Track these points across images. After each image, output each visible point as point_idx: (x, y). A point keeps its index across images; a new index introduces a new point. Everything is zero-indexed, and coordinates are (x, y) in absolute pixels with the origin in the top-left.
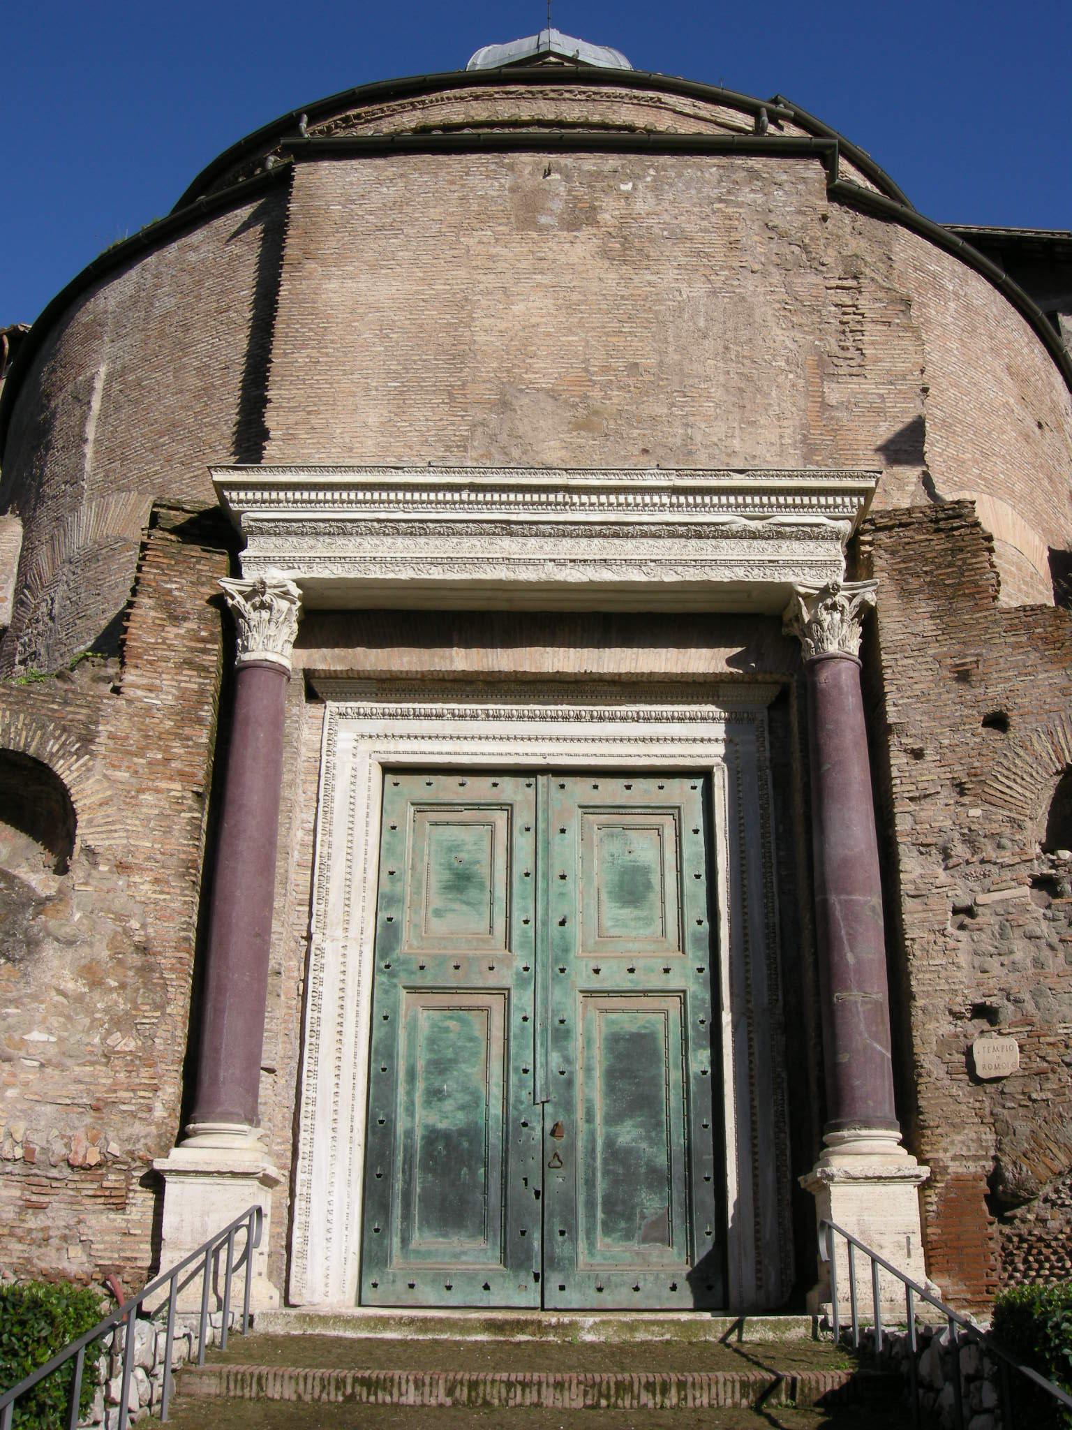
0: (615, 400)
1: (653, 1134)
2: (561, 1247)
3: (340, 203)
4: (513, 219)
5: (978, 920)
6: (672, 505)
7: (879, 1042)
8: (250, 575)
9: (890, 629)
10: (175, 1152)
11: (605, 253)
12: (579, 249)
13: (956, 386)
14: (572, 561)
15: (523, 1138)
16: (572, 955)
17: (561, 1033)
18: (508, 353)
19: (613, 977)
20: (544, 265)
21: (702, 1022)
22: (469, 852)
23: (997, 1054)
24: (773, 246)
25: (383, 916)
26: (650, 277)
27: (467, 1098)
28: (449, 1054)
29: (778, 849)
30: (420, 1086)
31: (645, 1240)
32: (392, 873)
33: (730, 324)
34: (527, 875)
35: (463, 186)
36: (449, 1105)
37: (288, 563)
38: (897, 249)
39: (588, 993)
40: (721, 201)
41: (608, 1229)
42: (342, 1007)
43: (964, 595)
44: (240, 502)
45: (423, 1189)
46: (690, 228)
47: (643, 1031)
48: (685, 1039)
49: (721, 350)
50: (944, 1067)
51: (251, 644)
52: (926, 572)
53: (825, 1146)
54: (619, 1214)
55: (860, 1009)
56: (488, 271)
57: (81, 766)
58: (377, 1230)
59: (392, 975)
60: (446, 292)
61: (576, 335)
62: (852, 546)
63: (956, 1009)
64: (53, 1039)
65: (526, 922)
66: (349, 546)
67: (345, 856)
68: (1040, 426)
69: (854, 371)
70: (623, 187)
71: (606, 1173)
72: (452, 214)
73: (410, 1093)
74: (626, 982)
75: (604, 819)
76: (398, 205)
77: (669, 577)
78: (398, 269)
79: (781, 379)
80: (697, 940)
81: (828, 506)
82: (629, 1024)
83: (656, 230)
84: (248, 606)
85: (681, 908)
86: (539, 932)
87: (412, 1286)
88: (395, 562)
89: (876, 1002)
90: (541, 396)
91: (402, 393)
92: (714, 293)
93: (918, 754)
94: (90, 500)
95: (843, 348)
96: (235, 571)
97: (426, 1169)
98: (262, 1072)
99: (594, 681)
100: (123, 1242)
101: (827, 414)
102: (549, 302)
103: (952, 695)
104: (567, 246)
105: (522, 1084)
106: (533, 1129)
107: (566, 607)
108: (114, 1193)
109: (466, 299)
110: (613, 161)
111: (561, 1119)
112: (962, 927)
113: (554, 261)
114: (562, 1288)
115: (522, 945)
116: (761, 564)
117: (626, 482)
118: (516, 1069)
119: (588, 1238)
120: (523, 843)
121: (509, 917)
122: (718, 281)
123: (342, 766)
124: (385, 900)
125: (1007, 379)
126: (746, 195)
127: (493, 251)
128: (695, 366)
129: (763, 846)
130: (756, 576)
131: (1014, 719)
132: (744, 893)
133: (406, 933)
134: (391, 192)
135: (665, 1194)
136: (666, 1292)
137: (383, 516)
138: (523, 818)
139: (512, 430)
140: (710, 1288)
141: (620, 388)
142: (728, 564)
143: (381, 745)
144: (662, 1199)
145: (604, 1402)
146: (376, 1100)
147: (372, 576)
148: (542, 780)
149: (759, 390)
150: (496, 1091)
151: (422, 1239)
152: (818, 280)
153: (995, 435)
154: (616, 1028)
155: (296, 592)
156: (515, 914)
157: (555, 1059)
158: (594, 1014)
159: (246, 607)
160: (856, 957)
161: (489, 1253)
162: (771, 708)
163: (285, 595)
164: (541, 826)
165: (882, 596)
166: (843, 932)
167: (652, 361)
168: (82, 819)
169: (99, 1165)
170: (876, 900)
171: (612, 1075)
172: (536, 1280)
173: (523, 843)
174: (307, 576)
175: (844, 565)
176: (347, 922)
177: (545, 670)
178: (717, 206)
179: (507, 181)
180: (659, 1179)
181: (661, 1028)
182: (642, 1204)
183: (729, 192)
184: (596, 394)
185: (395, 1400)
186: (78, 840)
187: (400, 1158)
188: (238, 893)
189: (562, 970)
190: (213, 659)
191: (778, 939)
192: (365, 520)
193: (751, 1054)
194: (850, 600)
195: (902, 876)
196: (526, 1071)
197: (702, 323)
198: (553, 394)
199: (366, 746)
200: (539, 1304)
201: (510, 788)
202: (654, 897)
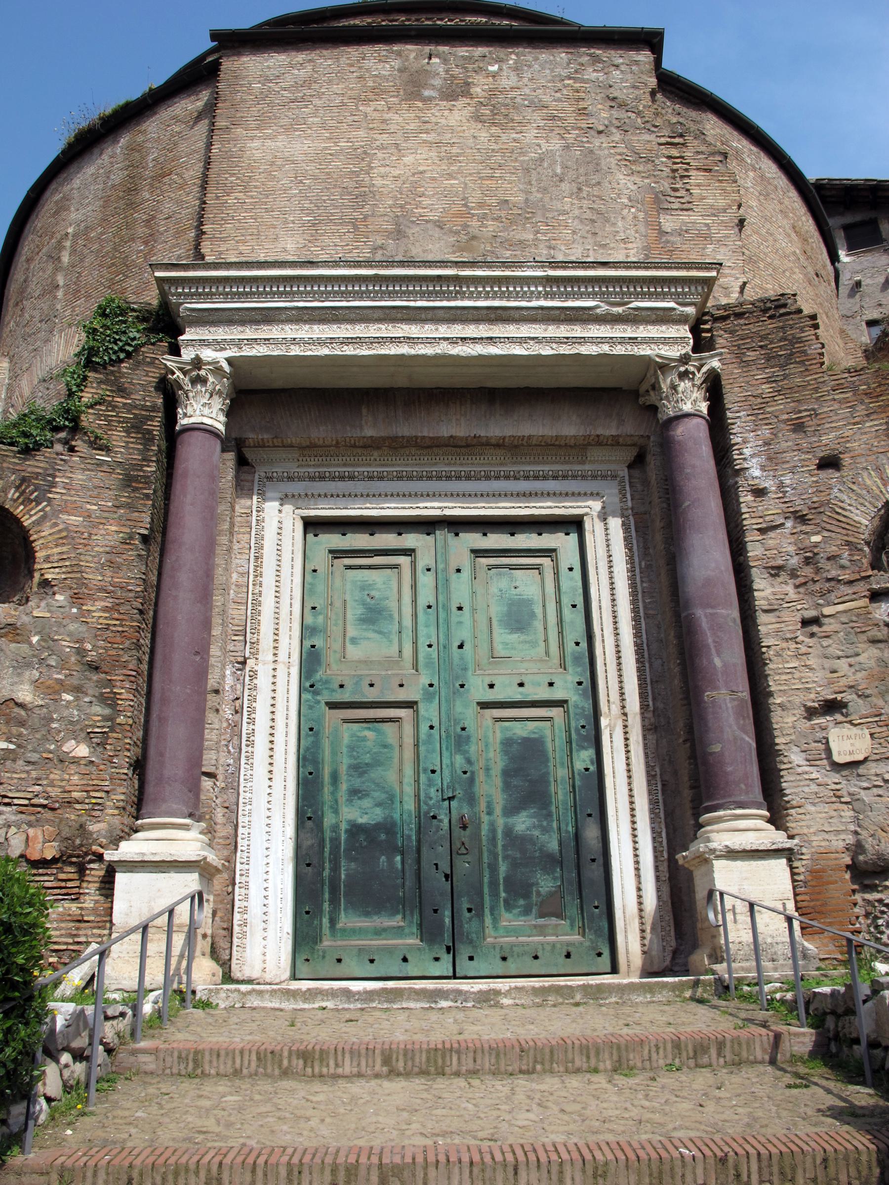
1: (545, 823)
2: (469, 925)
3: (259, 82)
4: (402, 93)
5: (825, 628)
6: (547, 293)
7: (746, 733)
8: (187, 354)
9: (732, 397)
10: (123, 845)
11: (477, 118)
12: (457, 115)
13: (757, 233)
14: (462, 339)
15: (433, 830)
16: (470, 673)
18: (401, 194)
19: (506, 691)
20: (428, 126)
21: (583, 727)
22: (379, 590)
23: (848, 742)
24: (615, 113)
25: (307, 644)
26: (514, 135)
27: (384, 796)
28: (367, 758)
29: (642, 582)
30: (344, 787)
31: (542, 915)
32: (314, 608)
33: (582, 171)
34: (429, 607)
35: (360, 68)
36: (366, 803)
37: (219, 345)
39: (484, 705)
40: (570, 78)
41: (509, 906)
42: (273, 720)
43: (796, 362)
44: (180, 295)
45: (346, 875)
46: (546, 99)
47: (533, 736)
48: (570, 742)
49: (575, 190)
50: (803, 755)
51: (189, 410)
52: (761, 347)
53: (701, 826)
54: (518, 891)
55: (729, 705)
56: (383, 131)
57: (40, 511)
58: (307, 913)
59: (316, 693)
60: (350, 147)
61: (455, 179)
62: (695, 330)
63: (810, 704)
64: (12, 747)
65: (430, 646)
66: (275, 332)
67: (274, 594)
68: (817, 275)
69: (685, 206)
70: (490, 68)
71: (505, 858)
72: (352, 89)
73: (333, 793)
74: (517, 695)
76: (308, 83)
77: (546, 351)
80: (577, 659)
81: (678, 294)
82: (521, 730)
83: (518, 100)
84: (187, 379)
85: (561, 633)
86: (441, 654)
87: (339, 961)
88: (312, 342)
89: (742, 700)
91: (314, 225)
92: (568, 147)
94: (61, 331)
95: (675, 190)
96: (175, 351)
97: (350, 859)
98: (204, 778)
99: (482, 445)
100: (78, 929)
101: (664, 239)
102: (433, 154)
103: (790, 444)
104: (446, 113)
106: (441, 821)
107: (458, 383)
108: (69, 884)
109: (365, 153)
110: (481, 50)
111: (466, 811)
112: (812, 635)
113: (437, 124)
114: (471, 958)
115: (428, 665)
116: (623, 341)
117: (508, 273)
118: (425, 770)
119: (492, 914)
120: (426, 581)
121: (415, 643)
123: (271, 545)
124: (307, 631)
125: (793, 235)
126: (591, 74)
127: (386, 116)
128: (554, 202)
130: (619, 350)
131: (846, 460)
132: (615, 617)
134: (302, 74)
135: (558, 875)
136: (562, 959)
139: (406, 252)
140: (599, 955)
141: (494, 219)
144: (555, 879)
145: (539, 1067)
146: (304, 799)
147: (292, 353)
149: (607, 220)
150: (409, 790)
151: (347, 920)
152: (652, 137)
153: (787, 274)
154: (509, 734)
155: (226, 368)
157: (459, 760)
158: (489, 722)
159: (185, 381)
160: (723, 661)
161: (407, 931)
162: (630, 467)
163: (218, 370)
164: (441, 566)
165: (725, 367)
166: (710, 640)
167: (521, 198)
168: (40, 555)
169: (54, 860)
170: (735, 614)
171: (507, 773)
172: (448, 952)
173: (426, 581)
174: (238, 354)
175: (691, 341)
177: (440, 434)
179: (397, 63)
180: (551, 862)
181: (548, 733)
182: (538, 884)
183: (576, 72)
184: (475, 223)
185: (332, 1071)
186: (37, 575)
187: (327, 850)
188: (179, 617)
189: (462, 686)
190: (156, 425)
191: (646, 656)
192: (286, 308)
193: (628, 752)
195: (756, 594)
196: (433, 772)
197: (559, 171)
200: (451, 974)
201: (410, 540)
202: (538, 625)
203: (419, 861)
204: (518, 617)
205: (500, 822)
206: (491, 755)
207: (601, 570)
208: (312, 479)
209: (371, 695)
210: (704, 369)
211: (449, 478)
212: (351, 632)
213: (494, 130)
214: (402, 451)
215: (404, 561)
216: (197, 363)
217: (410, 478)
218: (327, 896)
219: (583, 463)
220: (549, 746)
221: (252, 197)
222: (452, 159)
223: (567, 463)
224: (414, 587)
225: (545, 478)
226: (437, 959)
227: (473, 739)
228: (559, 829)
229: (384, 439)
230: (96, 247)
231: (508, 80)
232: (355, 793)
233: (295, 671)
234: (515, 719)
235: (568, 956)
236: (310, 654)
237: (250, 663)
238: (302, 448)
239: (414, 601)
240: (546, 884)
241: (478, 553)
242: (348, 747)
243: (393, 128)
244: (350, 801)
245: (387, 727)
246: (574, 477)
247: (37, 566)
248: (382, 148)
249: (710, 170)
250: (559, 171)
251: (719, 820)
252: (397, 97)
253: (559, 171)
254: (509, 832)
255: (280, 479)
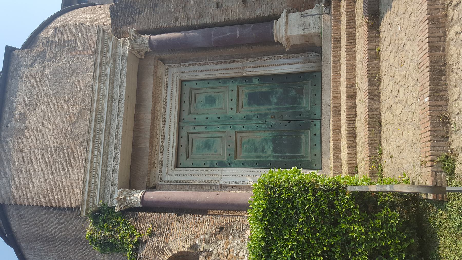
0: (77, 106)
11: (34, 110)
12: (32, 118)
16: (227, 115)
17: (248, 118)
19: (233, 104)
20: (35, 127)
25: (216, 166)
27: (264, 142)
28: (252, 147)
30: (261, 154)
33: (58, 75)
38: (44, 36)
39: (237, 111)
40: (22, 78)
41: (300, 104)
52: (128, 16)
54: (295, 101)
59: (232, 163)
73: (263, 157)
74: (235, 101)
75: (192, 109)
78: (32, 170)
79: (75, 62)
82: (246, 100)
90: (74, 127)
92: (49, 80)
93: (176, 20)
95: (68, 46)
105: (261, 127)
114: (315, 115)
118: (257, 129)
120: (198, 129)
121: (217, 132)
122: (45, 79)
124: (212, 166)
127: (30, 142)
129: (200, 65)
130: (126, 61)
133: (220, 160)
137: (101, 164)
138: (191, 129)
140: (315, 76)
141: (74, 105)
142: (122, 69)
143: (170, 168)
148: (181, 124)
150: (262, 134)
155: (121, 189)
156: (216, 130)
158: (243, 109)
163: (122, 193)
164: (193, 124)
168: (182, 249)
171: (259, 104)
173: (198, 129)
176: (217, 175)
178: (23, 80)
193: (254, 67)
194: (134, 36)
196: (257, 126)
198: (74, 124)
199: (170, 172)
201: (184, 133)
202: (213, 95)
203: (285, 131)
204: (211, 101)
205: (273, 106)
206: (253, 109)
207: (197, 74)
208: (162, 165)
209: (233, 146)
210: (134, 34)
211: (165, 121)
212: (213, 152)
213: (39, 105)
214: (155, 135)
215: (191, 136)
216: (119, 199)
217: (164, 133)
218: (295, 159)
219: (162, 78)
220: (251, 92)
221: (56, 189)
222: (49, 119)
223: (162, 83)
224: (199, 133)
225: (167, 91)
226: (315, 125)
227: (248, 114)
228: (276, 88)
229: (150, 140)
230: (67, 253)
231: (20, 99)
232: (263, 151)
233: (224, 169)
234: (242, 102)
235: (315, 85)
236: (219, 165)
237: (221, 183)
238: (151, 168)
239: (204, 133)
240: (293, 93)
241: (190, 113)
242: (249, 153)
243: (35, 140)
244: (266, 152)
245: (243, 141)
246: (167, 81)
247: (186, 250)
248: (42, 143)
249: (62, 33)
250: (57, 83)
251: (276, 34)
252: (22, 139)
253: (57, 83)
254: (276, 104)
255: (161, 175)
